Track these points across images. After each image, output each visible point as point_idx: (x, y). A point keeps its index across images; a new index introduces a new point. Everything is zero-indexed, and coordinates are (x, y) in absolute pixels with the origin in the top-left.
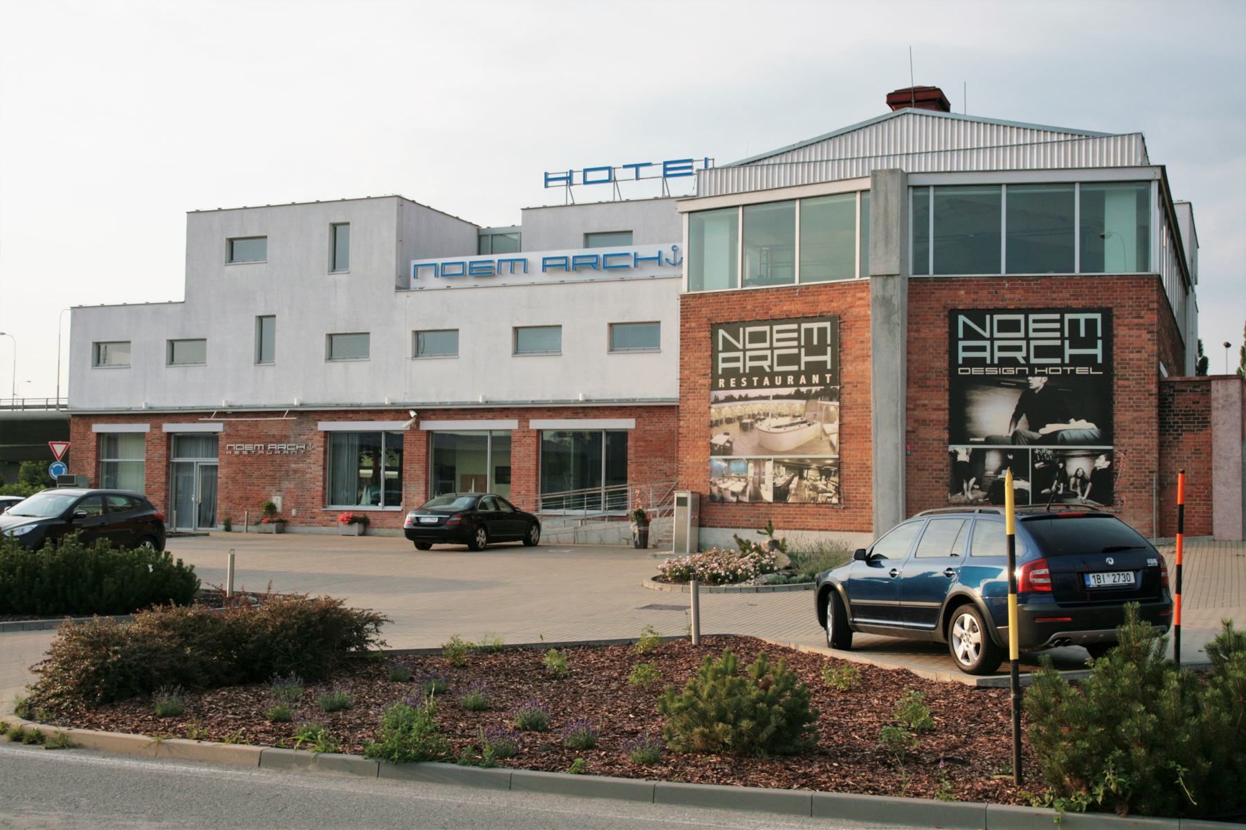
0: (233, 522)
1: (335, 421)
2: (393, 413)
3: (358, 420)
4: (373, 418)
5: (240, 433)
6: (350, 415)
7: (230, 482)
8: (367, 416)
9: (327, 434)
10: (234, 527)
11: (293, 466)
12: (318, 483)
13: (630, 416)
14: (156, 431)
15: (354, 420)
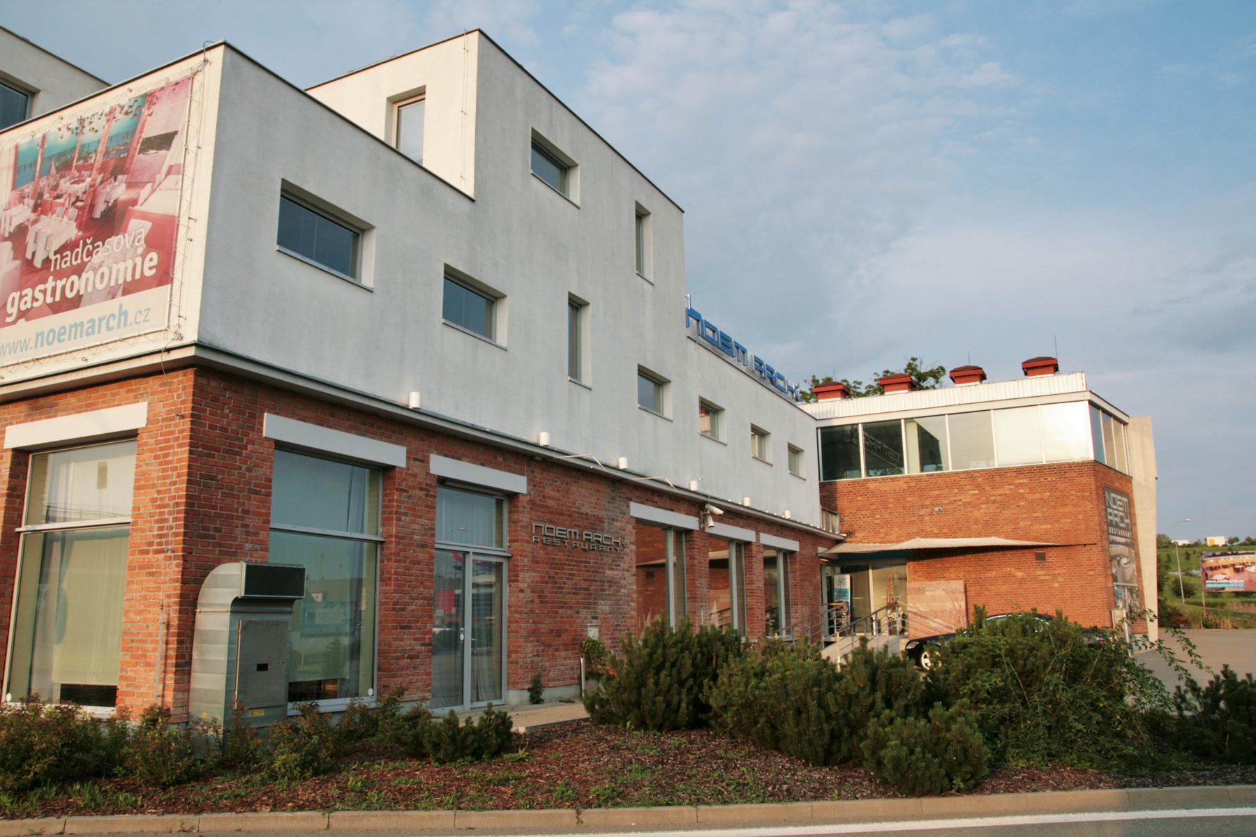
0: (543, 681)
1: (644, 503)
2: (687, 504)
3: (663, 508)
4: (673, 507)
5: (550, 503)
6: (656, 499)
7: (537, 600)
8: (668, 504)
9: (640, 522)
10: (546, 694)
11: (608, 572)
12: (633, 604)
13: (795, 539)
14: (417, 468)
15: (659, 507)
